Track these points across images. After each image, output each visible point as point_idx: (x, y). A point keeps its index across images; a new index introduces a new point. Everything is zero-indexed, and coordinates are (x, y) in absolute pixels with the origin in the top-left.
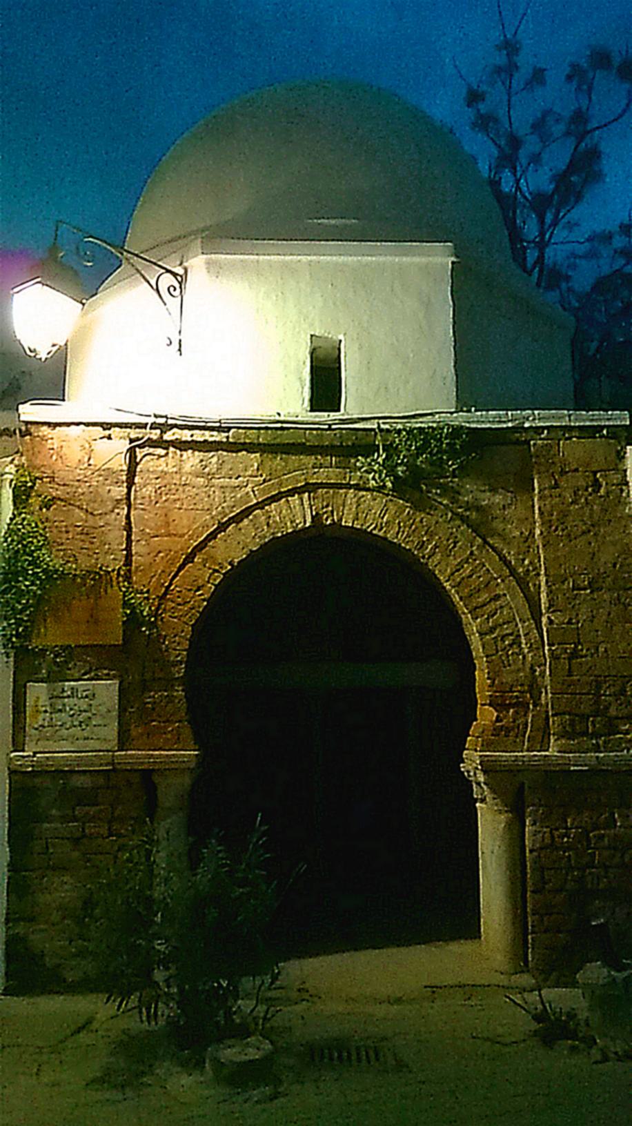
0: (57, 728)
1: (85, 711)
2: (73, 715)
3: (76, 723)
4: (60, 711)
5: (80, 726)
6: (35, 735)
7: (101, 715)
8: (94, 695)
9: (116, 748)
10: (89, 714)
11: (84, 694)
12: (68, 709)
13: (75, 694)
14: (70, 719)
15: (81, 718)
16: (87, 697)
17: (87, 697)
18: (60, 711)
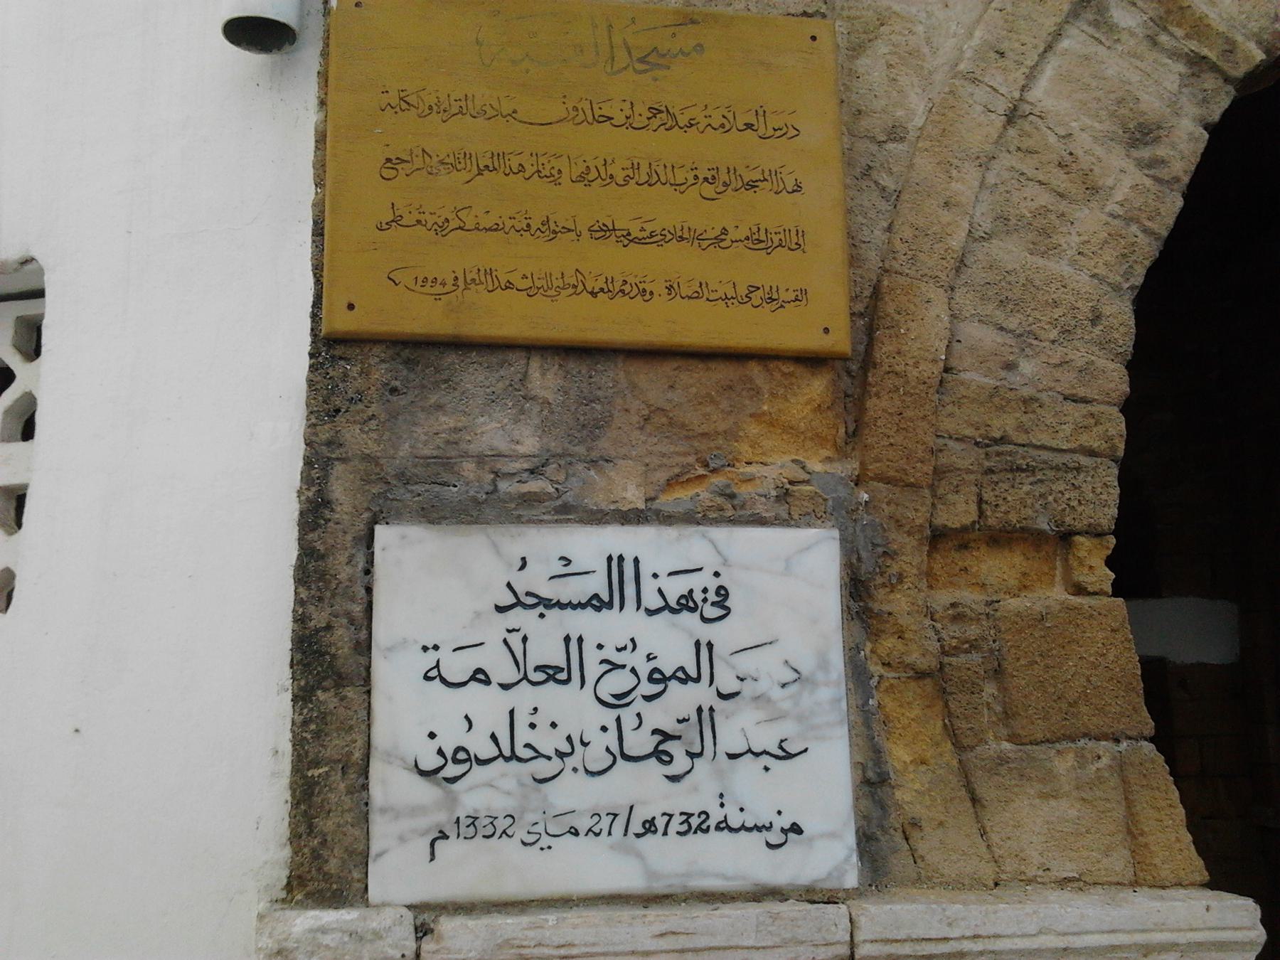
0: (543, 768)
1: (683, 677)
2: (621, 699)
3: (640, 742)
4: (552, 674)
5: (660, 755)
6: (416, 811)
7: (760, 699)
8: (722, 592)
9: (851, 880)
10: (700, 694)
11: (675, 588)
12: (593, 670)
13: (630, 590)
14: (609, 717)
15: (661, 715)
16: (687, 603)
17: (687, 603)
18: (552, 674)
